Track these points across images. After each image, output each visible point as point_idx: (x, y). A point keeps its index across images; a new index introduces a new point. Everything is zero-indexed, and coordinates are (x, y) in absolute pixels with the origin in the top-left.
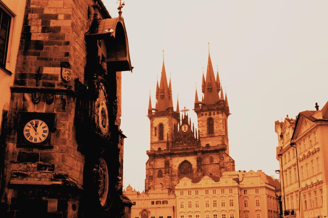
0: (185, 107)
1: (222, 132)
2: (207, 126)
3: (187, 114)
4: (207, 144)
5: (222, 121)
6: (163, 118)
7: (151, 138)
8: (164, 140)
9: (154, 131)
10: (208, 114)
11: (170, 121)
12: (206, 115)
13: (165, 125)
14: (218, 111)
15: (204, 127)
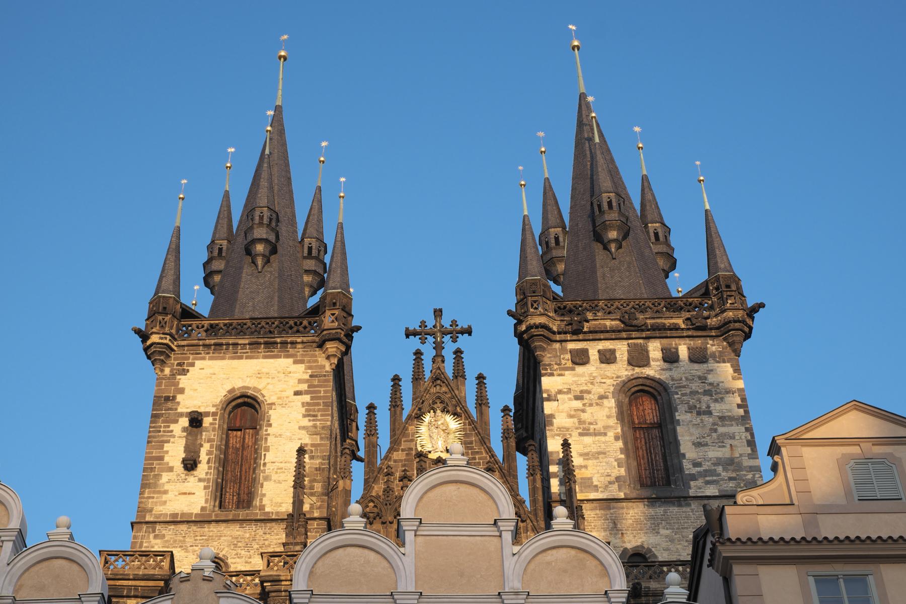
0: (438, 313)
1: (750, 476)
2: (619, 430)
3: (458, 353)
4: (629, 546)
5: (739, 406)
6: (261, 360)
7: (144, 486)
8: (257, 502)
9: (183, 441)
10: (625, 358)
11: (316, 383)
12: (607, 358)
13: (273, 404)
14: (699, 342)
15: (595, 435)
